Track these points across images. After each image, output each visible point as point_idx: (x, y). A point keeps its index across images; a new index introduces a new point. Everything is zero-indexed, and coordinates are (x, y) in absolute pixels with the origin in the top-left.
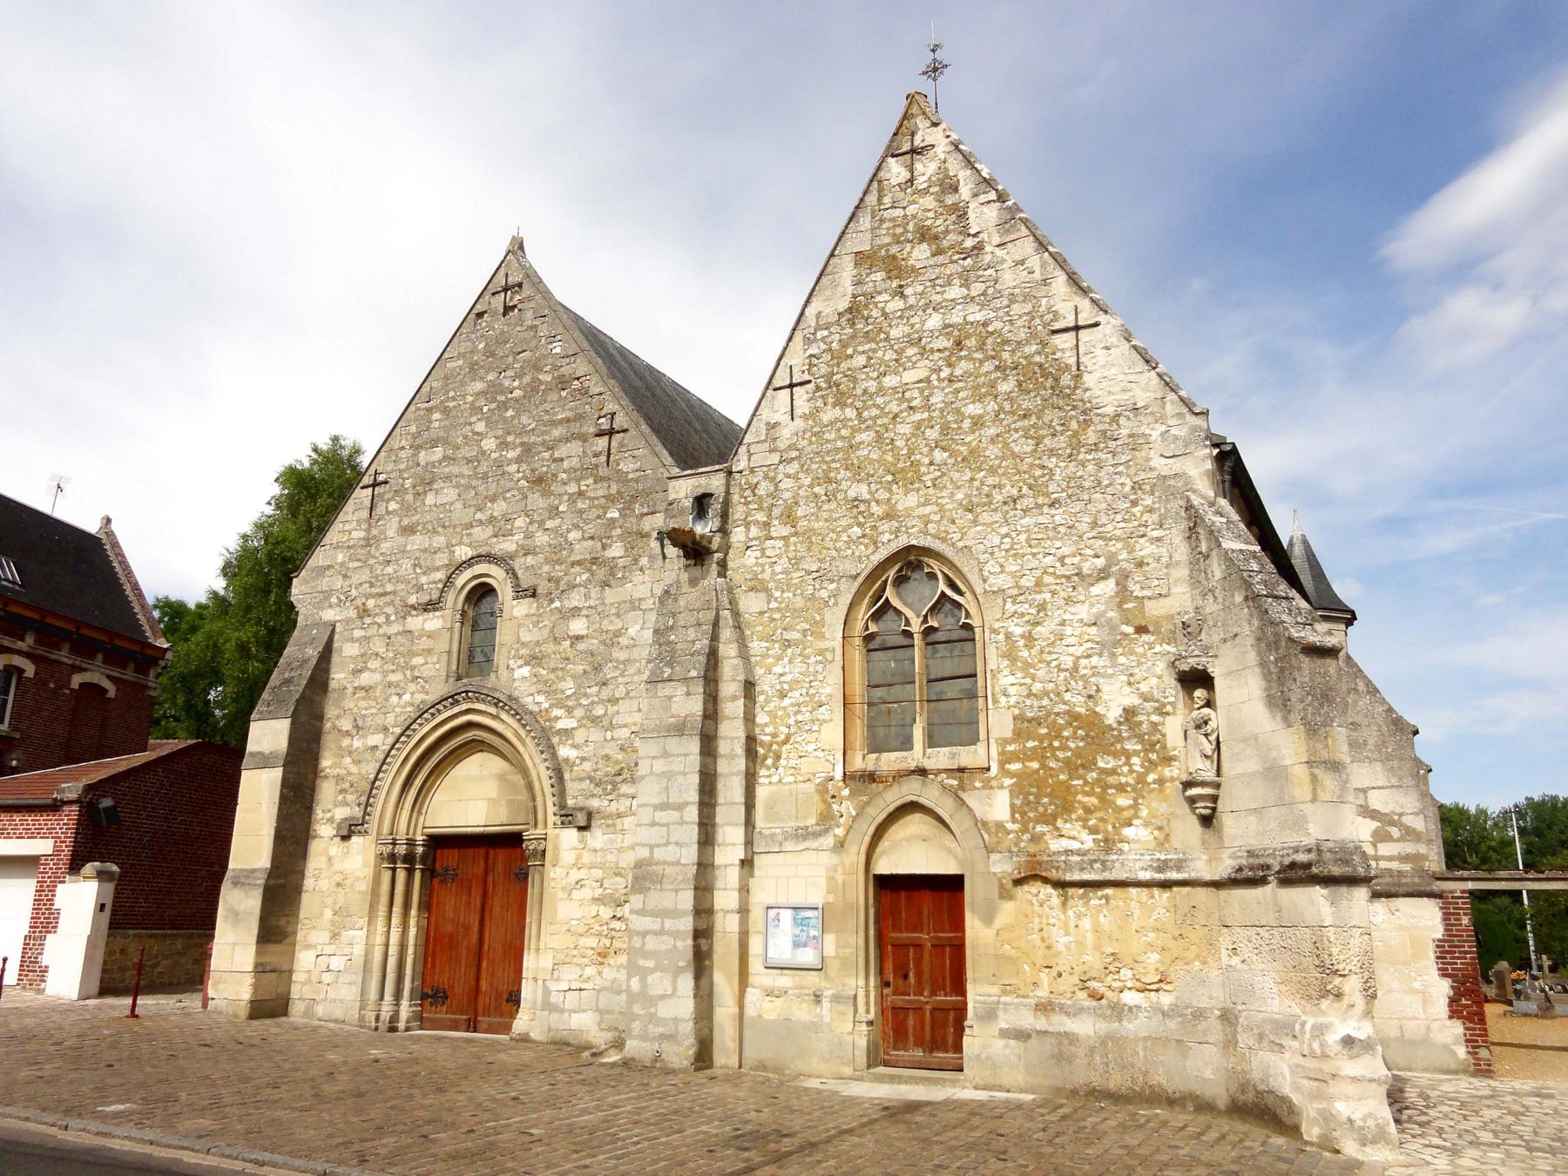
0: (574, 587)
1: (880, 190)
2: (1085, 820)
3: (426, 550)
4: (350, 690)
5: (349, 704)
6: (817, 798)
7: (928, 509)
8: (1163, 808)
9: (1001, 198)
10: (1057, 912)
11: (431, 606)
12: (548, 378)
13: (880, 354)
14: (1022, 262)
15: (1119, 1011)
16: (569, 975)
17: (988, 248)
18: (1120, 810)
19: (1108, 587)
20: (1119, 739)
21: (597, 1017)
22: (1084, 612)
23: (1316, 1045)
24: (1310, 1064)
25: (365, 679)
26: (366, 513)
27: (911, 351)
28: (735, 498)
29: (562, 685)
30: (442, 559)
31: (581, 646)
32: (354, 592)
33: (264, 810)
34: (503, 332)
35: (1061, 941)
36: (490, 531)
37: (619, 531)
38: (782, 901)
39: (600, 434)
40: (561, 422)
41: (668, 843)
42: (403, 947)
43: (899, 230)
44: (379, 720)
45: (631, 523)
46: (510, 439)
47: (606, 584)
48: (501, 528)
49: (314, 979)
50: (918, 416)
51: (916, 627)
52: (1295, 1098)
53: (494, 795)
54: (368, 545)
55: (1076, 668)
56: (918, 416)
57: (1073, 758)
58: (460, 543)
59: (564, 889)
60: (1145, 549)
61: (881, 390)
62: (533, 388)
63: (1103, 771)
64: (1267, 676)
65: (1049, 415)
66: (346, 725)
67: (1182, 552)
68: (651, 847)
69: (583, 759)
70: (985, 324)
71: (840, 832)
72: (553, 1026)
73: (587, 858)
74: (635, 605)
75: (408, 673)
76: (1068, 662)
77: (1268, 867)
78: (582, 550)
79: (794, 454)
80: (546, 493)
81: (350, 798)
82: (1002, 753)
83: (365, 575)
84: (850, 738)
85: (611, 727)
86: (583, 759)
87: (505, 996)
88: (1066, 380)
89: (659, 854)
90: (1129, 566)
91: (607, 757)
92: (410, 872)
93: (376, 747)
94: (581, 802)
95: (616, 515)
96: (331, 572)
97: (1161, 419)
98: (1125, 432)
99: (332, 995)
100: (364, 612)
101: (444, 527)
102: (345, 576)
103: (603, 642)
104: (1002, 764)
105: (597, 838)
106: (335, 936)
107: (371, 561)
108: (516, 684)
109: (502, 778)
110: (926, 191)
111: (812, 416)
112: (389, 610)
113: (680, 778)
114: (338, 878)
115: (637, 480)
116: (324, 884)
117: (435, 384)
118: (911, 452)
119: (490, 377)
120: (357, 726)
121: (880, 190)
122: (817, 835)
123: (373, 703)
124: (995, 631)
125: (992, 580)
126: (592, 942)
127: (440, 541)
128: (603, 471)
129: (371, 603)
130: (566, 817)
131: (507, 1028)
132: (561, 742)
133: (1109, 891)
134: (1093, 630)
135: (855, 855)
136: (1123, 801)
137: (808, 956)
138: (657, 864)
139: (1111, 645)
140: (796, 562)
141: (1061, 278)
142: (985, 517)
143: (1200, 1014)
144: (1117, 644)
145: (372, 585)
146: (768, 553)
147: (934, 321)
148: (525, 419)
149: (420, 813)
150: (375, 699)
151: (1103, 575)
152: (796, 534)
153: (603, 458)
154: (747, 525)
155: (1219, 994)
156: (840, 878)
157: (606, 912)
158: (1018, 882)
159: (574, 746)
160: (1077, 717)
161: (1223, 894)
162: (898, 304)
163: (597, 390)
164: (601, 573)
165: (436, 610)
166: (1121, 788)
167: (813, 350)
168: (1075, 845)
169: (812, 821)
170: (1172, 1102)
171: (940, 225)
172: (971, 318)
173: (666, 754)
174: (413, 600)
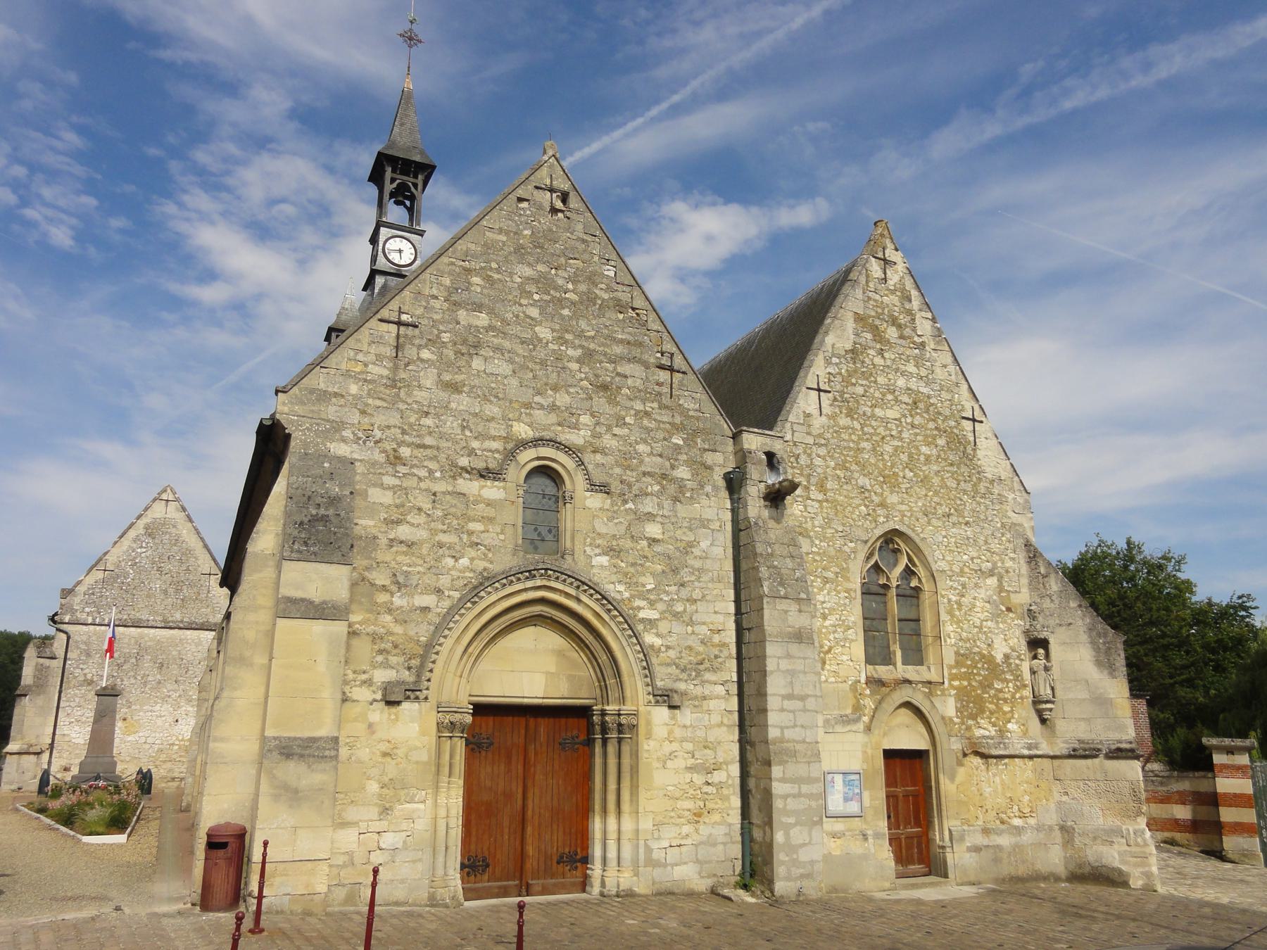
0: (647, 494)
1: (867, 276)
4: (383, 541)
5: (383, 555)
6: (851, 695)
7: (904, 507)
8: (1024, 714)
9: (934, 320)
10: (984, 773)
11: (485, 474)
12: (606, 296)
13: (872, 390)
14: (945, 366)
15: (1018, 830)
16: (670, 834)
18: (1005, 713)
19: (992, 582)
20: (1004, 672)
21: (696, 868)
22: (982, 594)
23: (1139, 840)
24: (1134, 849)
25: (403, 532)
26: (389, 352)
27: (890, 397)
29: (642, 579)
30: (496, 429)
31: (658, 548)
32: (378, 434)
33: (321, 667)
34: (551, 230)
35: (988, 790)
36: (553, 418)
37: (685, 457)
38: (834, 768)
39: (661, 367)
40: (622, 341)
41: (795, 726)
43: (880, 310)
44: (429, 580)
45: (694, 452)
46: (569, 337)
47: (676, 500)
51: (894, 583)
52: (1124, 868)
53: (553, 670)
54: (394, 387)
55: (981, 628)
56: (896, 443)
57: (980, 681)
58: (519, 420)
60: (1009, 564)
61: (873, 415)
62: (590, 299)
63: (997, 690)
64: (1097, 649)
65: (963, 469)
66: (381, 578)
67: (1024, 569)
68: (782, 728)
69: (668, 647)
70: (929, 397)
71: (866, 719)
72: (657, 880)
73: (678, 733)
74: (704, 523)
75: (465, 537)
76: (978, 623)
77: (1099, 750)
78: (652, 463)
79: (823, 442)
80: (612, 401)
81: (393, 660)
82: (950, 674)
83: (395, 419)
85: (691, 623)
86: (668, 647)
88: (969, 450)
89: (789, 734)
90: (1003, 571)
91: (690, 648)
93: (426, 609)
94: (668, 684)
96: (342, 401)
97: (1012, 490)
101: (497, 397)
102: (363, 412)
104: (951, 680)
105: (686, 716)
106: (385, 811)
107: (402, 406)
108: (595, 571)
109: (560, 653)
110: (893, 292)
111: (832, 417)
112: (433, 465)
113: (801, 676)
114: (384, 747)
115: (698, 419)
116: (364, 753)
117: (473, 247)
118: (892, 466)
119: (541, 268)
120: (398, 583)
121: (867, 276)
124: (943, 596)
125: (939, 563)
126: (689, 804)
127: (493, 410)
128: (666, 400)
129: (405, 452)
131: (584, 885)
132: (645, 630)
133: (1006, 760)
136: (1006, 708)
137: (854, 807)
138: (788, 741)
139: (995, 616)
140: (828, 522)
141: (966, 386)
142: (934, 521)
143: (1051, 828)
144: (999, 616)
145: (404, 432)
146: (809, 509)
148: (583, 324)
151: (991, 573)
152: (827, 501)
153: (666, 390)
155: (1054, 816)
156: (870, 751)
157: (699, 779)
158: (965, 755)
159: (658, 635)
160: (983, 656)
161: (1057, 762)
162: (878, 360)
163: (655, 328)
164: (672, 489)
168: (987, 733)
169: (849, 711)
170: (1045, 878)
171: (903, 319)
172: (921, 389)
173: (789, 656)
174: (464, 462)
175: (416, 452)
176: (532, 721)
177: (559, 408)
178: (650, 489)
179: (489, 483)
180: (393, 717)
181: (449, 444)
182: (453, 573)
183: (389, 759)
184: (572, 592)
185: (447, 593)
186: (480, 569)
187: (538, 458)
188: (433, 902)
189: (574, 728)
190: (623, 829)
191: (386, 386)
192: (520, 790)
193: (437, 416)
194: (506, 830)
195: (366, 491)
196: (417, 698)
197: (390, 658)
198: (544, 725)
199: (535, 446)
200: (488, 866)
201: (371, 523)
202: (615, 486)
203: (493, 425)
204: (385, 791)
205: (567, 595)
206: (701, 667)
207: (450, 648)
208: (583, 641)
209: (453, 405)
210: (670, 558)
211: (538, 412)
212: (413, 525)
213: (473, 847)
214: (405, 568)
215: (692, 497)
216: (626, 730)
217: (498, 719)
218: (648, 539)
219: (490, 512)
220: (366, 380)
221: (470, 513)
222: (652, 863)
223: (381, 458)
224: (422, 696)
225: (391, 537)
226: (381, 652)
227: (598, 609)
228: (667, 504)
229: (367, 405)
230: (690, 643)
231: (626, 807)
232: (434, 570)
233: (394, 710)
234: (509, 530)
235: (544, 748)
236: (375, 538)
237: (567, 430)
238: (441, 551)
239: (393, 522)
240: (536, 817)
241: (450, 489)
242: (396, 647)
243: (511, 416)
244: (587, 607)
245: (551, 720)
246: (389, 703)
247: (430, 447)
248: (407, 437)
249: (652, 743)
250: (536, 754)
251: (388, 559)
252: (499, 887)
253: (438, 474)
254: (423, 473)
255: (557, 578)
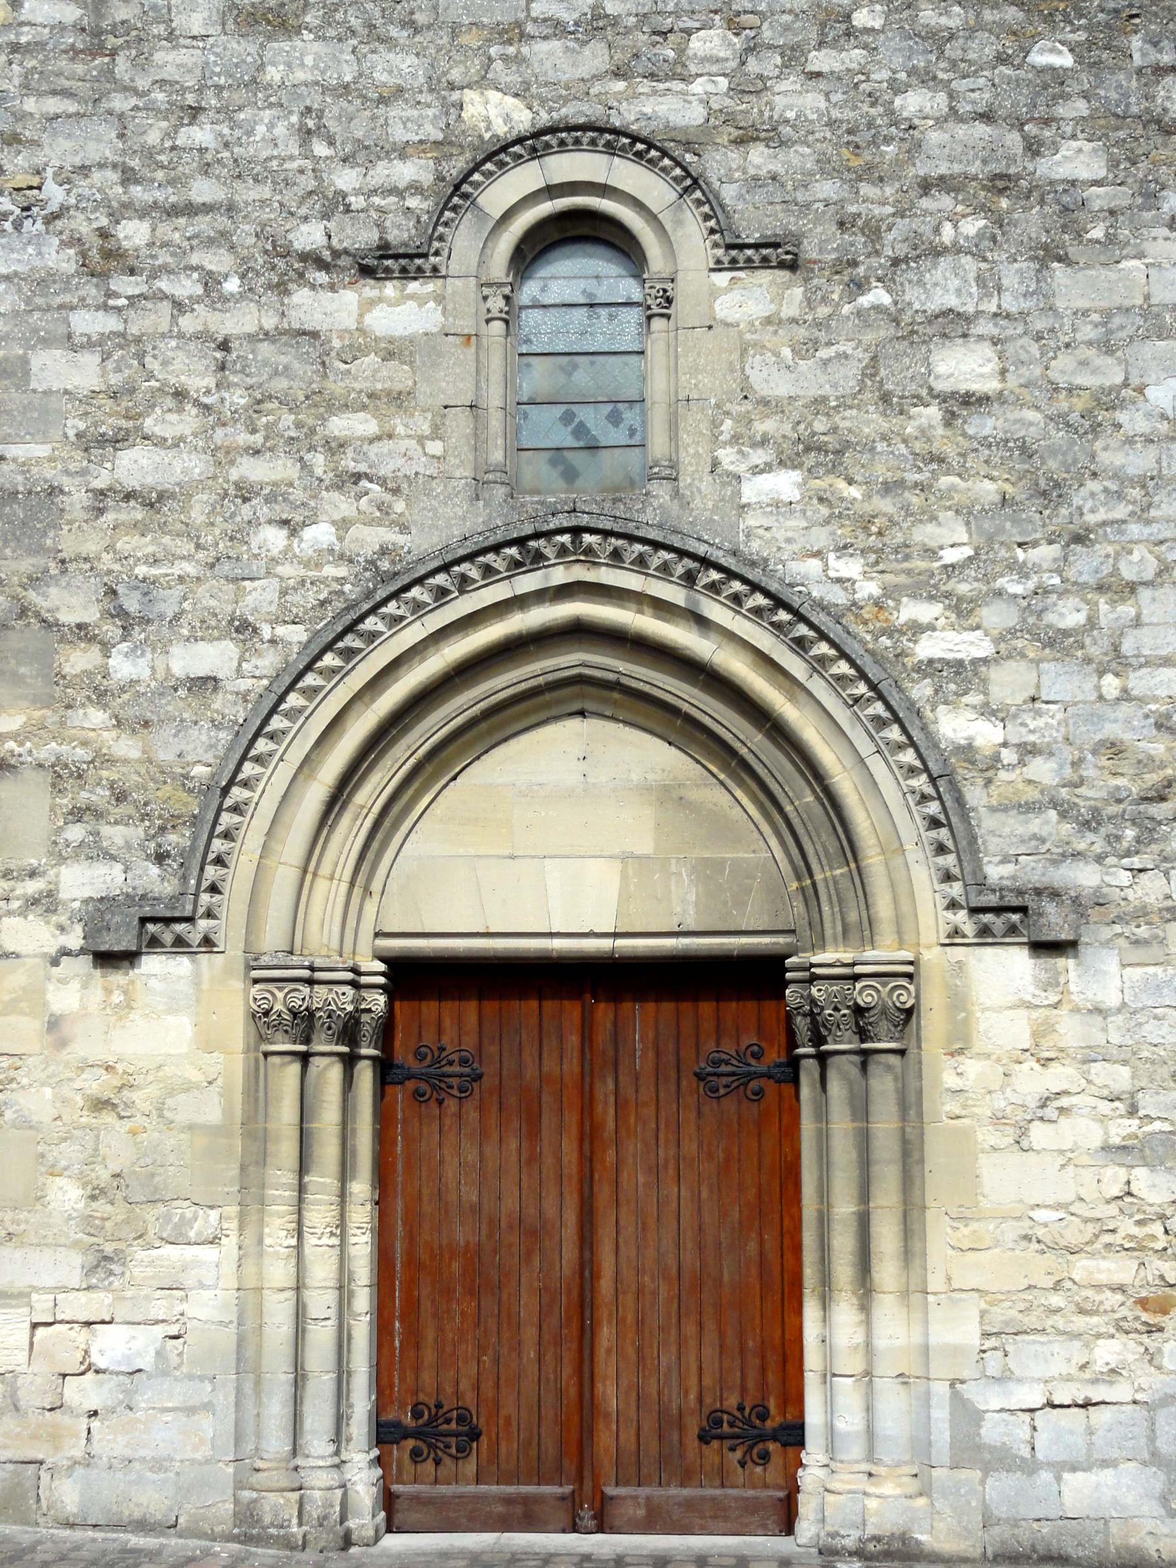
0: (937, 252)
3: (345, 89)
4: (77, 499)
5: (80, 539)
11: (382, 263)
16: (1044, 1367)
21: (1156, 1480)
25: (135, 466)
29: (925, 534)
31: (983, 425)
32: (54, 194)
36: (595, 57)
37: (1081, 107)
42: (344, 1290)
44: (214, 597)
45: (1119, 87)
47: (1048, 255)
49: (32, 1394)
53: (646, 847)
54: (95, 50)
58: (482, 82)
59: (998, 1119)
66: (74, 604)
69: (1028, 751)
72: (1001, 1511)
73: (1071, 1031)
75: (319, 461)
78: (950, 147)
81: (115, 835)
83: (101, 143)
86: (1028, 751)
87: (693, 1427)
91: (1115, 749)
92: (349, 1061)
93: (206, 684)
94: (1033, 872)
95: (1066, 60)
99: (110, 1441)
103: (1060, 419)
105: (1103, 975)
107: (120, 103)
108: (752, 520)
109: (668, 796)
112: (216, 261)
114: (95, 1084)
120: (121, 613)
123: (188, 547)
126: (1121, 1269)
127: (397, 65)
129: (133, 233)
130: (1008, 916)
145: (129, 177)
149: (367, 892)
150: (188, 532)
159: (987, 711)
164: (1032, 222)
165: (405, 275)
174: (310, 236)
175: (166, 230)
176: (604, 1012)
177: (615, 21)
178: (948, 231)
179: (390, 289)
180: (117, 998)
181: (265, 191)
182: (285, 570)
183: (108, 1118)
184: (674, 594)
185: (266, 632)
186: (368, 551)
187: (551, 191)
188: (249, 1527)
189: (729, 1032)
190: (881, 1343)
191: (74, 53)
192: (571, 1217)
193: (227, 113)
194: (530, 1333)
195: (25, 362)
196: (179, 941)
197: (106, 830)
198: (643, 1023)
199: (535, 154)
200: (475, 1435)
201: (41, 451)
202: (820, 242)
203: (397, 111)
204: (102, 1207)
205: (661, 607)
206: (1159, 810)
207: (284, 794)
208: (733, 753)
209: (273, 74)
210: (1026, 452)
211: (542, 47)
212: (161, 442)
213: (427, 1377)
214: (142, 570)
215: (1111, 239)
216: (885, 1026)
217: (491, 1007)
218: (943, 398)
219: (398, 376)
220: (15, 48)
221: (336, 386)
222: (972, 1452)
223: (64, 261)
224: (195, 938)
225: (99, 484)
226: (77, 814)
227: (764, 640)
228: (1014, 275)
229: (22, 117)
230: (1112, 730)
231: (886, 1271)
232: (226, 568)
233: (118, 978)
234: (459, 424)
235: (647, 1093)
236: (54, 491)
237: (645, 86)
238: (246, 511)
239: (103, 441)
240: (629, 1300)
241: (270, 322)
242: (120, 797)
243: (456, 75)
244: (728, 641)
245: (668, 1007)
246: (106, 959)
247: (207, 208)
248: (136, 191)
249: (972, 1067)
250: (620, 1105)
251: (91, 547)
252: (508, 1501)
253: (232, 285)
254: (186, 287)
255: (616, 555)
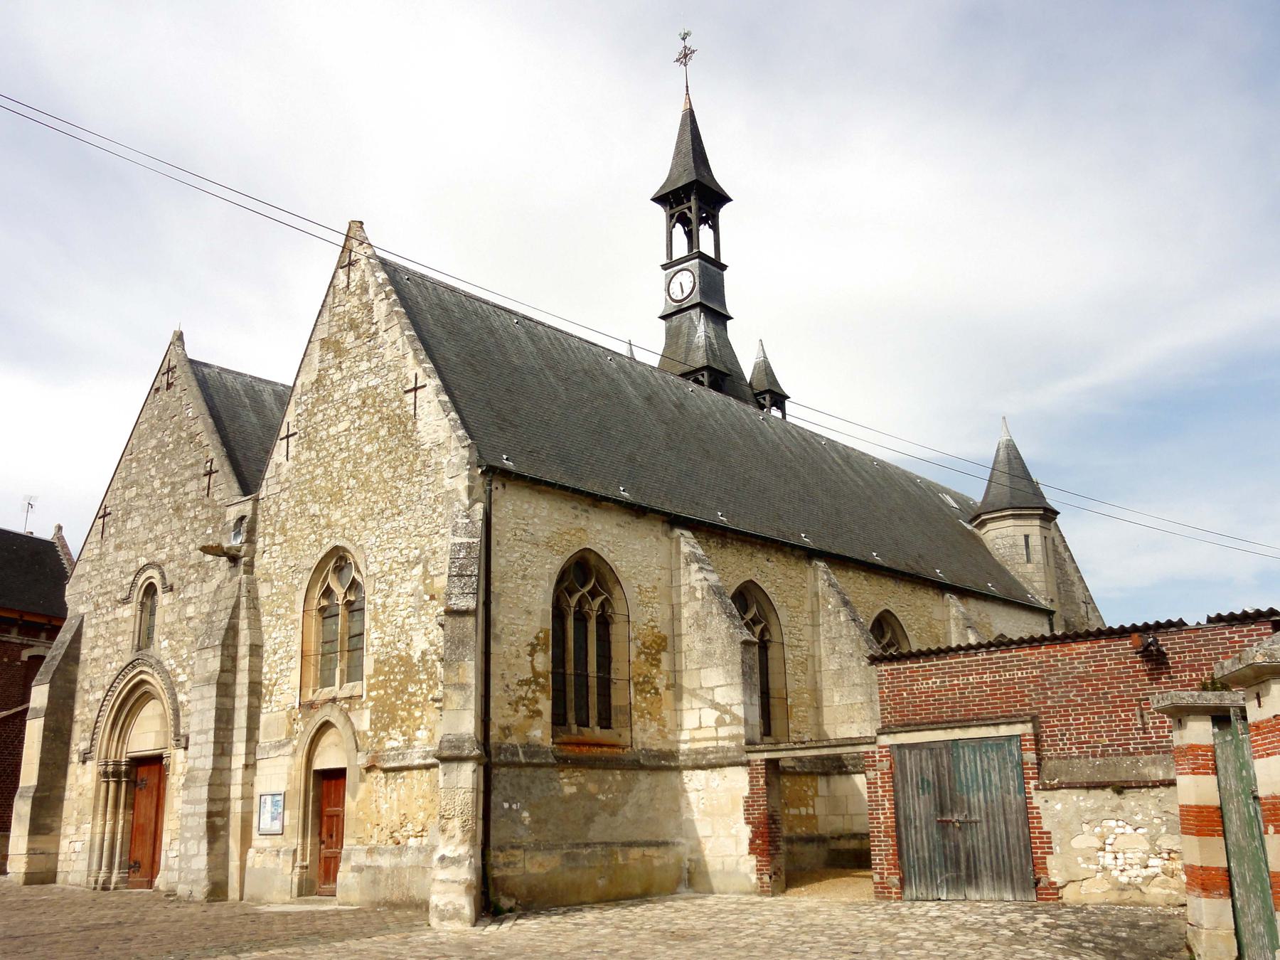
2: (401, 727)
11: (126, 601)
17: (381, 333)
18: (416, 719)
19: (418, 570)
22: (409, 587)
28: (260, 518)
30: (133, 567)
47: (204, 581)
48: (158, 541)
50: (345, 455)
65: (401, 451)
66: (87, 686)
80: (180, 518)
84: (305, 680)
92: (118, 783)
98: (433, 461)
100: (97, 607)
104: (368, 692)
106: (78, 828)
118: (340, 481)
122: (284, 745)
128: (206, 501)
133: (405, 773)
134: (412, 599)
135: (301, 759)
137: (277, 826)
144: (421, 608)
147: (354, 388)
154: (264, 536)
162: (337, 376)
166: (417, 705)
167: (299, 411)
169: (284, 737)
171: (358, 316)
174: (119, 597)
